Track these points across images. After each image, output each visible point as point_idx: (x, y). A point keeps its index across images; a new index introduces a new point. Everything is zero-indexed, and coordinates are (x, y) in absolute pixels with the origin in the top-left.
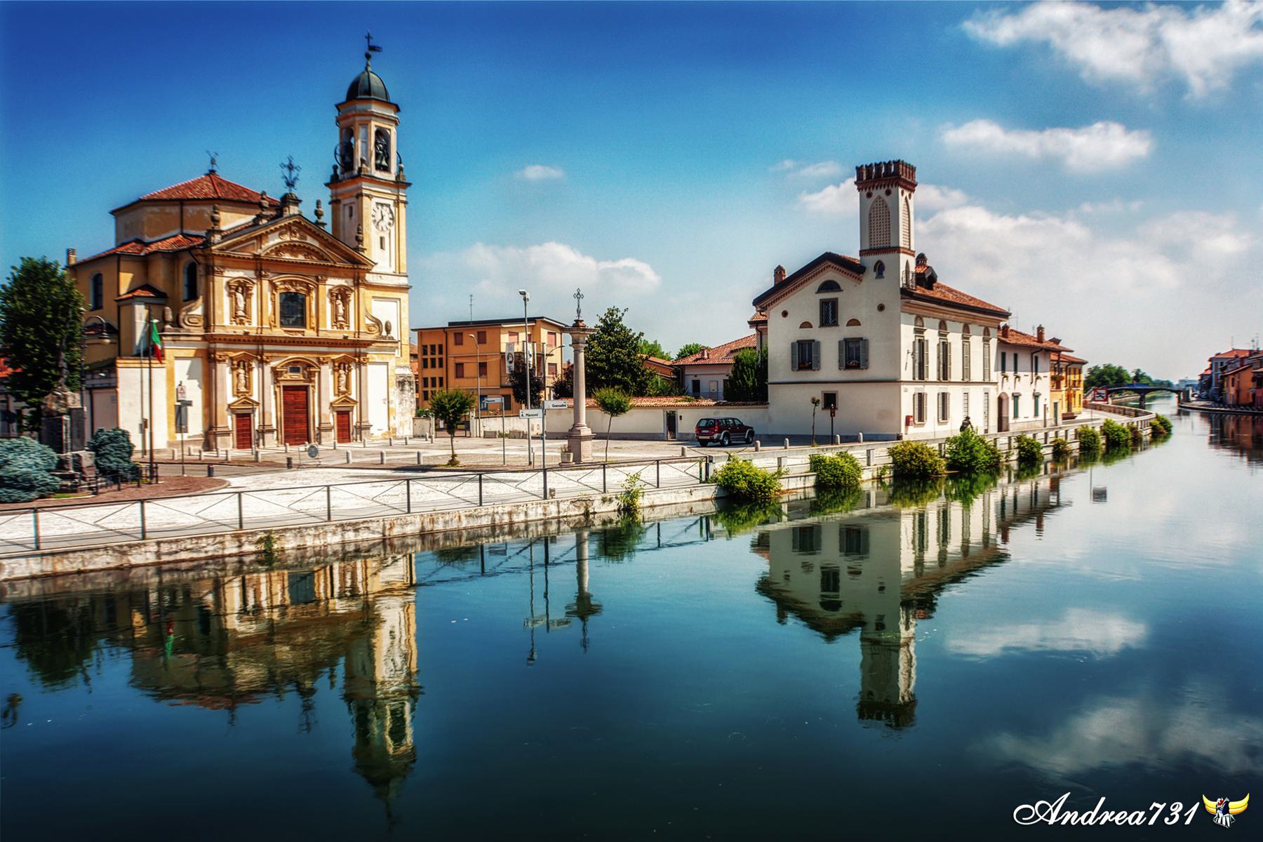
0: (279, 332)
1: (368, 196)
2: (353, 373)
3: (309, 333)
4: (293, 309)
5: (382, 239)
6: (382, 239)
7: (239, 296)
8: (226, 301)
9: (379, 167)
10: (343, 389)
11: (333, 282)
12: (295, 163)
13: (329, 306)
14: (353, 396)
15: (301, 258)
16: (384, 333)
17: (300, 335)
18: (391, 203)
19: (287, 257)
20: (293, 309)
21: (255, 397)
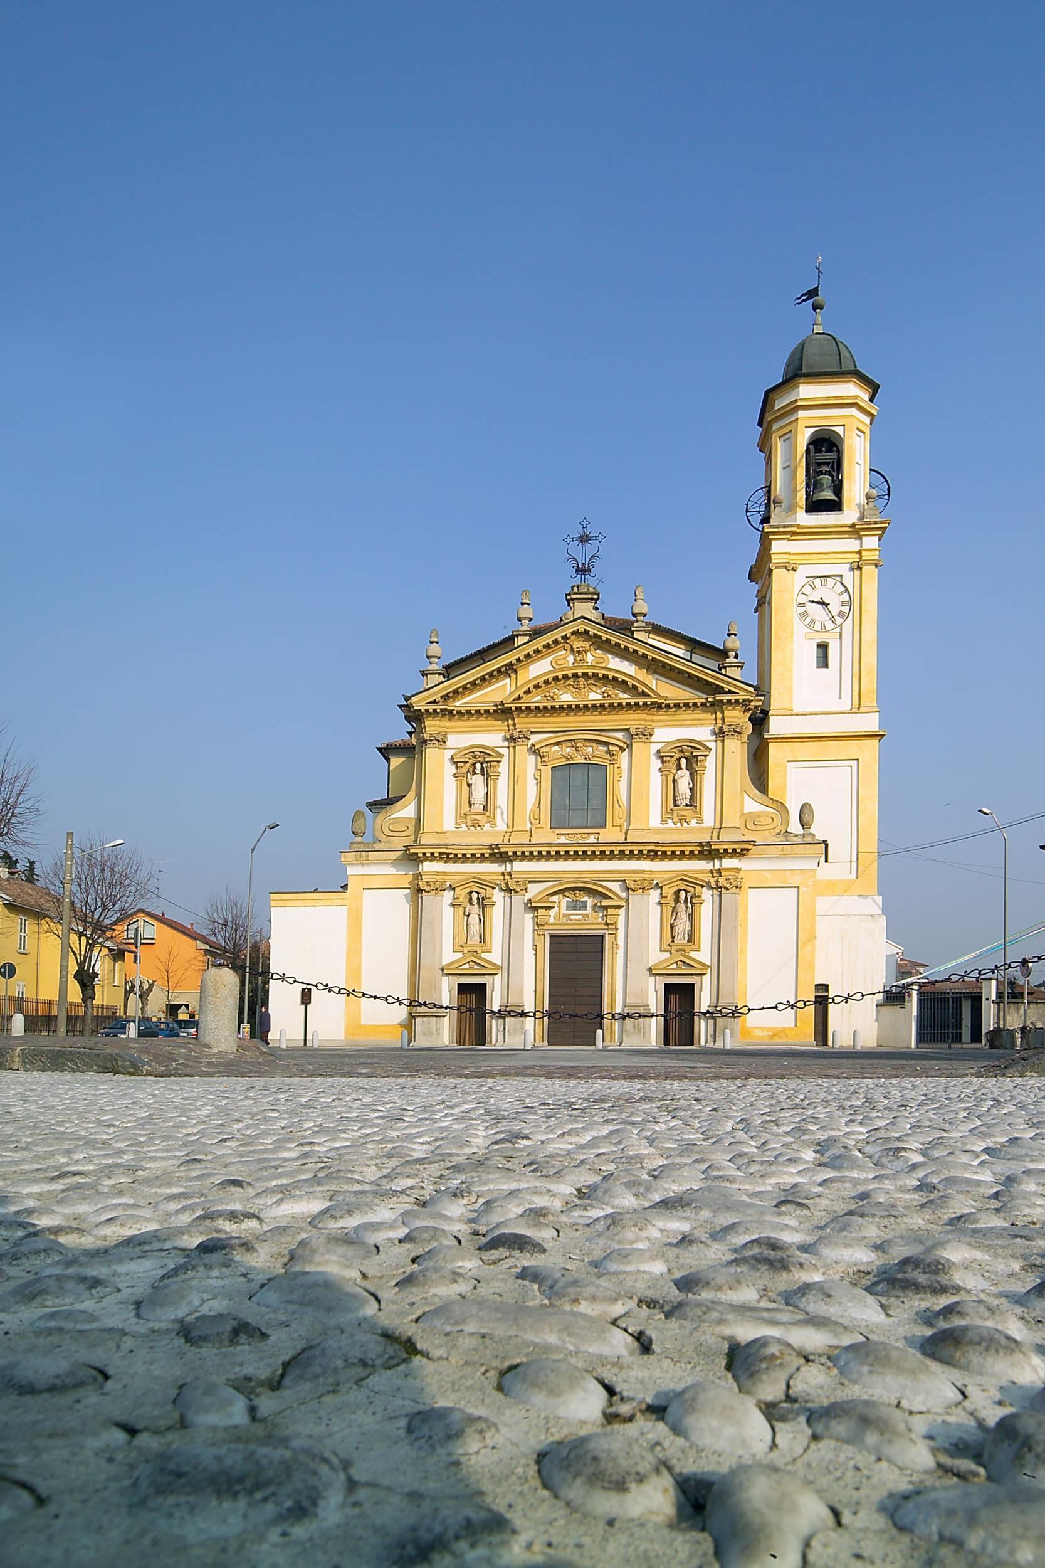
0: (546, 836)
2: (706, 912)
3: (610, 834)
4: (580, 793)
8: (449, 787)
9: (814, 506)
10: (681, 940)
11: (668, 733)
12: (592, 531)
13: (656, 779)
14: (704, 954)
15: (595, 696)
16: (795, 827)
17: (592, 839)
18: (844, 569)
19: (566, 697)
20: (580, 793)
21: (495, 956)
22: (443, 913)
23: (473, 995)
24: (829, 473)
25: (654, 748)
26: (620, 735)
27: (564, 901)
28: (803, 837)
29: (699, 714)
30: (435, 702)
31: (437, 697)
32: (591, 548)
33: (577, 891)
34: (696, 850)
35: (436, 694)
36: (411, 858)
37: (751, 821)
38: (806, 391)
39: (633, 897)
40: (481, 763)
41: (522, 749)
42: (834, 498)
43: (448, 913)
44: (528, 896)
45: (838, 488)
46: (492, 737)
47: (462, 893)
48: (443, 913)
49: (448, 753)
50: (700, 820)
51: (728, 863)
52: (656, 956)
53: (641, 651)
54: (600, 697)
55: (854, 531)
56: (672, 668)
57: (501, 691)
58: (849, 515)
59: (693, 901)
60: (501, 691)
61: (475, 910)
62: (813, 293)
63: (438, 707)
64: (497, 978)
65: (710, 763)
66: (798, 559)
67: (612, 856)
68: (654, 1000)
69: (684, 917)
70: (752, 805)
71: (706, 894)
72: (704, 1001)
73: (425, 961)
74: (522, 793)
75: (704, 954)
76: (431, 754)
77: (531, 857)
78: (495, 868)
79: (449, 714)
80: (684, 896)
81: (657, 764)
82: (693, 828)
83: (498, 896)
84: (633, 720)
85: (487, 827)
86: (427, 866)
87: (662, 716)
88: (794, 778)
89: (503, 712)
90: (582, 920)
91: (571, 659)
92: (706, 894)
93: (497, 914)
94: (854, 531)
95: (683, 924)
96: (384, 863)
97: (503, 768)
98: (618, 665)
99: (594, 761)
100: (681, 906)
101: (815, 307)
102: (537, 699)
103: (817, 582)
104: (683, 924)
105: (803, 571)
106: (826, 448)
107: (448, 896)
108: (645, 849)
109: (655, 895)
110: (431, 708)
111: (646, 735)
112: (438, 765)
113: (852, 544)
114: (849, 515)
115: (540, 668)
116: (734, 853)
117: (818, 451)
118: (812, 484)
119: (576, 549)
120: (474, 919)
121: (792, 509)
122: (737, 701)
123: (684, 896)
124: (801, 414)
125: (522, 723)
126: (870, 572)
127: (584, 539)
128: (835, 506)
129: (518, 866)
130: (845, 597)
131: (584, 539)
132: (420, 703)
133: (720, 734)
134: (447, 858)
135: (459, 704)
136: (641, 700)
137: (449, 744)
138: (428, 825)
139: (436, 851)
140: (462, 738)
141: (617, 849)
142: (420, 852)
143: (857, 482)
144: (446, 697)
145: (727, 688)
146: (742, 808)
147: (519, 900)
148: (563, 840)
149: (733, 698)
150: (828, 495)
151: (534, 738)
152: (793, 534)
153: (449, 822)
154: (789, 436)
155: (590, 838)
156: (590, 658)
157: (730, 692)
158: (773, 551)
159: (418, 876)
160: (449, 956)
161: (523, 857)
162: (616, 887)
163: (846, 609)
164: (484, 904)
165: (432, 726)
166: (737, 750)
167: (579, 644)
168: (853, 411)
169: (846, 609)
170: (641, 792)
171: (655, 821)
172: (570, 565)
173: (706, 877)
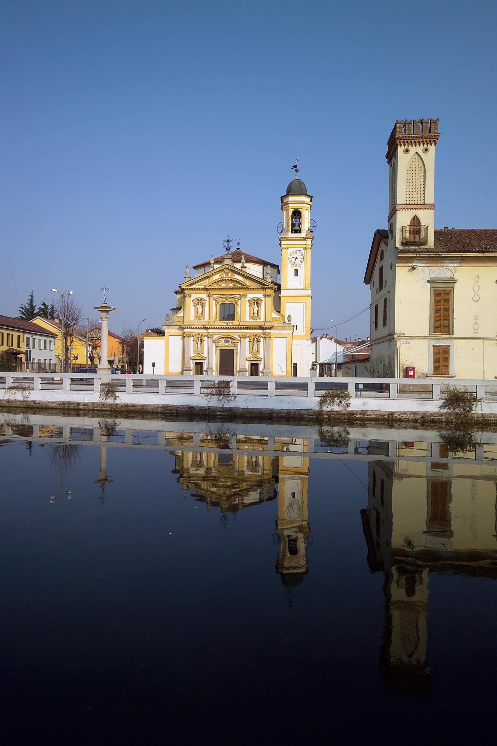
2: (261, 344)
6: (296, 270)
7: (200, 307)
8: (192, 309)
11: (251, 295)
13: (248, 308)
14: (261, 355)
15: (231, 285)
17: (231, 324)
18: (302, 249)
19: (223, 285)
21: (205, 355)
22: (191, 342)
23: (199, 365)
25: (247, 299)
26: (238, 296)
27: (223, 340)
28: (287, 324)
29: (259, 291)
32: (230, 244)
33: (227, 338)
34: (259, 327)
35: (188, 284)
36: (182, 328)
37: (274, 320)
38: (291, 199)
39: (242, 340)
40: (200, 302)
41: (211, 299)
43: (192, 343)
44: (214, 339)
46: (203, 295)
47: (196, 338)
48: (191, 342)
49: (192, 299)
50: (260, 319)
51: (267, 331)
52: (248, 355)
53: (243, 274)
55: (304, 239)
57: (206, 283)
59: (258, 341)
60: (206, 283)
61: (200, 342)
62: (295, 166)
63: (189, 287)
64: (206, 361)
65: (263, 304)
66: (289, 246)
67: (236, 329)
68: (248, 367)
69: (256, 345)
70: (275, 315)
71: (262, 339)
72: (261, 368)
73: (186, 356)
74: (212, 311)
75: (261, 355)
76: (187, 299)
77: (214, 328)
78: (205, 331)
80: (255, 339)
81: (248, 304)
83: (206, 339)
84: (242, 292)
85: (202, 320)
86: (186, 330)
87: (250, 291)
89: (206, 289)
90: (229, 345)
91: (224, 275)
92: (262, 339)
93: (205, 343)
94: (304, 239)
95: (255, 347)
96: (175, 329)
97: (207, 304)
100: (255, 342)
101: (297, 171)
102: (215, 286)
104: (255, 347)
105: (290, 249)
106: (297, 214)
107: (192, 338)
108: (245, 327)
109: (248, 339)
111: (245, 296)
112: (189, 304)
113: (304, 242)
114: (303, 234)
115: (216, 277)
116: (268, 329)
117: (295, 215)
118: (293, 225)
119: (226, 244)
120: (199, 344)
121: (288, 231)
123: (255, 339)
124: (290, 205)
125: (211, 292)
126: (309, 250)
127: (228, 241)
128: (299, 231)
129: (211, 331)
130: (302, 257)
131: (228, 241)
132: (183, 286)
133: (265, 296)
134: (191, 328)
135: (194, 286)
136: (243, 287)
137: (192, 297)
138: (186, 319)
139: (189, 326)
140: (195, 296)
141: (237, 327)
142: (184, 326)
143: (306, 224)
144: (191, 285)
146: (271, 316)
147: (211, 340)
148: (223, 324)
150: (297, 228)
151: (215, 296)
153: (192, 319)
154: (287, 210)
155: (231, 323)
156: (230, 274)
159: (184, 333)
160: (192, 354)
161: (212, 328)
162: (237, 337)
163: (302, 260)
164: (202, 341)
165: (187, 292)
166: (270, 301)
167: (227, 271)
168: (305, 205)
169: (302, 260)
170: (244, 311)
171: (248, 319)
172: (224, 248)
173: (261, 335)
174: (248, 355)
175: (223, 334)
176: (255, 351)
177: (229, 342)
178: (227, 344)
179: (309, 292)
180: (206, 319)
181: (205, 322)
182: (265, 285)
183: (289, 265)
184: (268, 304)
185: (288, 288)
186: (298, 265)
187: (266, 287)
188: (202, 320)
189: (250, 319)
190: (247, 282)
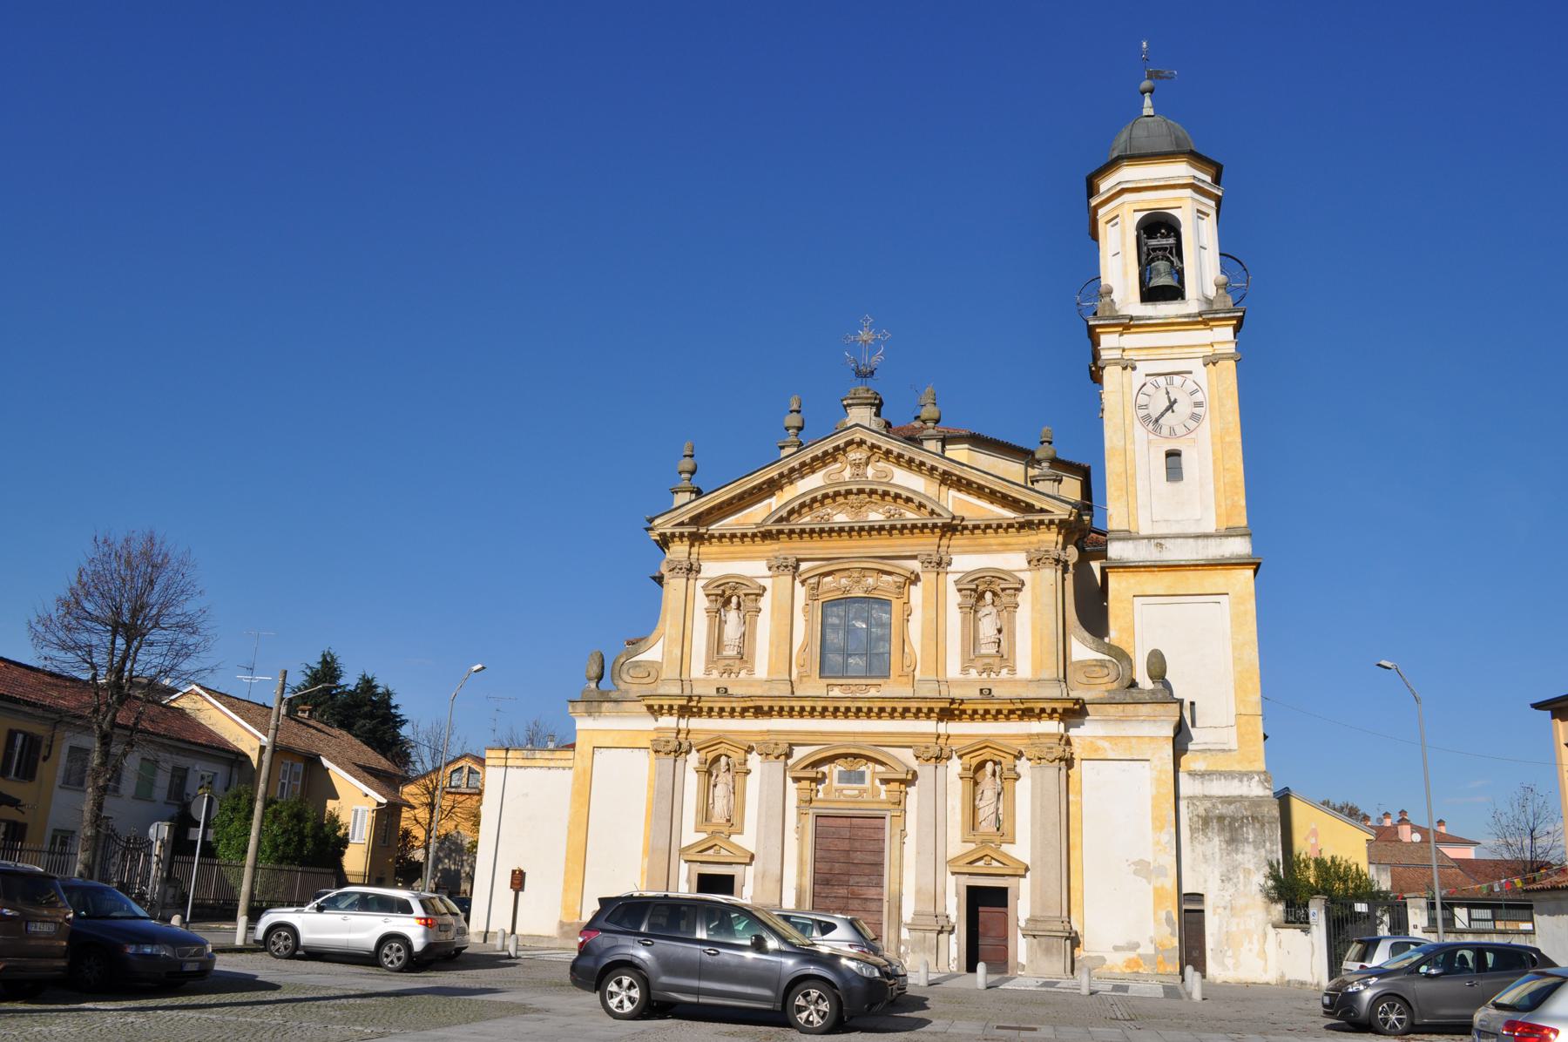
0: (814, 687)
1: (1115, 362)
3: (893, 688)
4: (854, 637)
5: (1173, 455)
9: (1150, 294)
11: (966, 561)
13: (954, 618)
15: (875, 516)
19: (841, 518)
20: (854, 637)
24: (1168, 259)
29: (1013, 538)
30: (682, 524)
31: (685, 518)
42: (1174, 283)
45: (1180, 274)
46: (752, 567)
54: (882, 517)
55: (1204, 320)
56: (970, 483)
58: (1191, 304)
70: (1082, 650)
74: (781, 632)
79: (696, 539)
82: (1002, 681)
84: (926, 544)
88: (1140, 619)
98: (904, 479)
99: (875, 594)
102: (806, 520)
103: (1161, 380)
106: (1158, 231)
110: (678, 530)
111: (940, 564)
114: (1191, 304)
122: (1051, 522)
128: (1175, 293)
135: (715, 528)
140: (715, 568)
144: (696, 520)
145: (1038, 505)
148: (836, 692)
149: (1046, 518)
150: (1163, 280)
152: (1128, 325)
157: (1042, 511)
158: (1103, 345)
170: (933, 634)
173: (1019, 745)
174: (956, 844)
175: (836, 740)
176: (987, 826)
177: (861, 777)
178: (851, 790)
179: (1240, 547)
180: (761, 670)
181: (751, 684)
182: (1029, 508)
183: (1140, 432)
184: (1041, 597)
185: (1143, 532)
186: (1180, 430)
187: (1036, 518)
188: (743, 674)
189: (965, 670)
190: (955, 502)
